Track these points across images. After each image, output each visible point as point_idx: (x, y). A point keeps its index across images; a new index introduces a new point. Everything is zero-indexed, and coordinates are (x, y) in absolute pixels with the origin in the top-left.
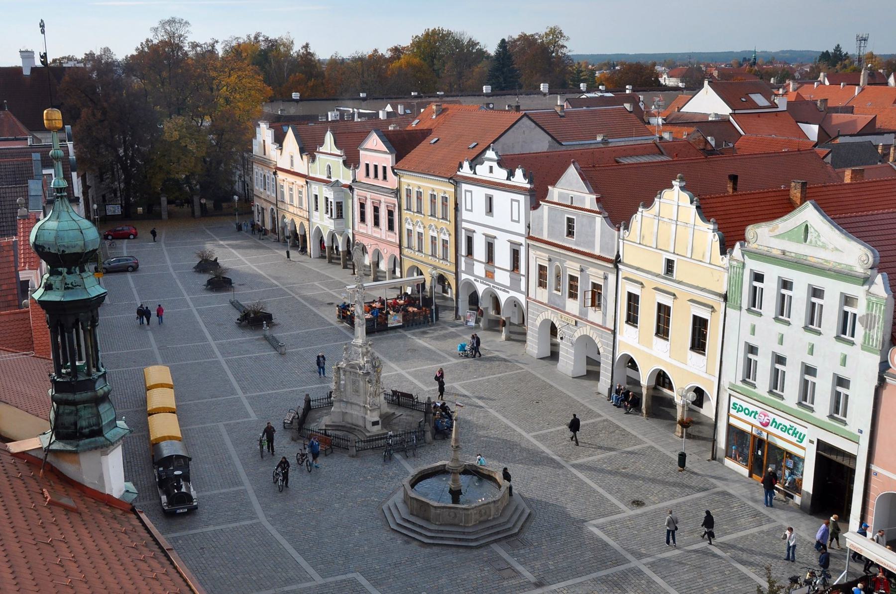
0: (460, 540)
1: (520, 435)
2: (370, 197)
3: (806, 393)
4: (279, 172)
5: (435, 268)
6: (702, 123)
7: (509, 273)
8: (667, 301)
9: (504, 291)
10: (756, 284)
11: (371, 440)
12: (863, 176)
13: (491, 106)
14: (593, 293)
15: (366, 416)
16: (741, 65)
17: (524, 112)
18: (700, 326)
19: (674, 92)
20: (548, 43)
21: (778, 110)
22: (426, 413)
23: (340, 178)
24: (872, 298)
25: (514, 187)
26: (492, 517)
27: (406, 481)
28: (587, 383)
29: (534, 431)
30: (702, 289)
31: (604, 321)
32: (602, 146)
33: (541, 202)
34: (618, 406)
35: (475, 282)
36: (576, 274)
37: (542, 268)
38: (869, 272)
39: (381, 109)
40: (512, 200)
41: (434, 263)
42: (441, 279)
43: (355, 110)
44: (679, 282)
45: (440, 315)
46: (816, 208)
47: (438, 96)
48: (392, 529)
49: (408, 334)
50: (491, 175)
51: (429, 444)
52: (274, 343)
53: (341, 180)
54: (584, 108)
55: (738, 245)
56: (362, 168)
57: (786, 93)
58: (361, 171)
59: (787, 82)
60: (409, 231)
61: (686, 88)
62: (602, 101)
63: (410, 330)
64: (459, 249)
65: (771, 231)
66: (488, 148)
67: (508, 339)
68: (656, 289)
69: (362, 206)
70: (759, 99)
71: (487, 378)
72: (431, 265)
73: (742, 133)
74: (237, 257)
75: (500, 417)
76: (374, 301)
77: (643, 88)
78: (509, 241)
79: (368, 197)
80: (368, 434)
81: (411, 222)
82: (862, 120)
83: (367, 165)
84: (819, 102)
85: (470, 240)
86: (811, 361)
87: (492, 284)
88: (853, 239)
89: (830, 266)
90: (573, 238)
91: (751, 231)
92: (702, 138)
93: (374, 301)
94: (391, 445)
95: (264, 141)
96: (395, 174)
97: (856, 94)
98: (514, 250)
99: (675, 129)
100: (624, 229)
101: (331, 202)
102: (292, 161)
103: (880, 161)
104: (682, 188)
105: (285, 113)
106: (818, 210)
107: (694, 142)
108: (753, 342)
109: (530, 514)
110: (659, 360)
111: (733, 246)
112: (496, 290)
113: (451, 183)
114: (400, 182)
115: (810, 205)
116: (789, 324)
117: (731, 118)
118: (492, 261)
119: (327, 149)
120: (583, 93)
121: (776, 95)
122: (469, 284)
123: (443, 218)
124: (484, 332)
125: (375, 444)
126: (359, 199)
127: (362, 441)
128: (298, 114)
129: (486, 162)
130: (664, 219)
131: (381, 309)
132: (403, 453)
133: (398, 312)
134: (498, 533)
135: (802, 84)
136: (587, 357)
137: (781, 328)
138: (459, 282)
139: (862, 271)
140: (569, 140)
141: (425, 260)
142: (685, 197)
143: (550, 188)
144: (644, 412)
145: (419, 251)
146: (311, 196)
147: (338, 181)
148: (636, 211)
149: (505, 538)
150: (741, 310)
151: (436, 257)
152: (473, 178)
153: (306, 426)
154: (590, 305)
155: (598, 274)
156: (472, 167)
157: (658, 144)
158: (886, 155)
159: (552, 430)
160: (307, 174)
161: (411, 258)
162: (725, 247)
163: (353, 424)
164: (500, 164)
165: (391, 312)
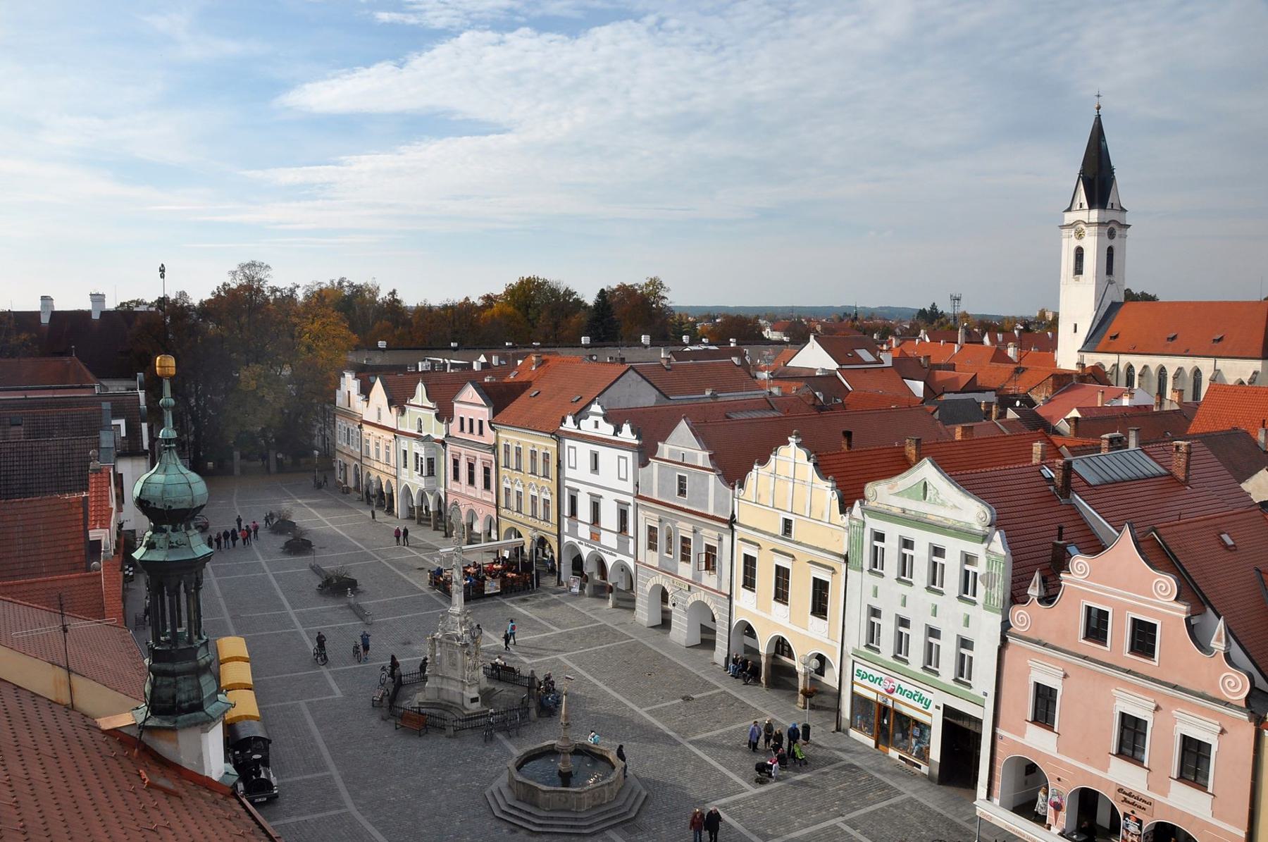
0: (572, 827)
2: (465, 453)
3: (931, 655)
4: (364, 425)
5: (536, 529)
6: (808, 377)
7: (616, 535)
8: (785, 563)
9: (611, 554)
10: (876, 543)
11: (470, 718)
12: (972, 434)
13: (594, 358)
15: (464, 692)
16: (842, 320)
17: (630, 364)
18: (820, 588)
19: (778, 346)
20: (649, 294)
21: (884, 365)
22: (529, 688)
23: (432, 432)
24: (991, 556)
26: (606, 801)
27: (511, 764)
28: (701, 652)
29: (648, 705)
31: (720, 585)
32: (712, 401)
33: (650, 459)
34: (735, 676)
35: (579, 545)
36: (689, 536)
38: (988, 530)
39: (475, 360)
40: (619, 457)
41: (535, 525)
42: (542, 542)
43: (446, 360)
44: (798, 543)
45: (541, 581)
46: (933, 465)
47: (534, 347)
48: (497, 817)
49: (507, 602)
50: (596, 430)
51: (534, 722)
54: (691, 361)
55: (857, 503)
56: (456, 423)
57: (890, 349)
58: (455, 425)
59: (890, 338)
60: (507, 490)
61: (791, 342)
63: (510, 597)
65: (889, 488)
66: (593, 401)
67: (615, 606)
68: (773, 550)
69: (456, 462)
70: (865, 354)
71: (594, 648)
72: (531, 527)
73: (850, 389)
75: (609, 691)
76: (469, 566)
78: (616, 500)
79: (463, 453)
80: (466, 712)
81: (509, 480)
82: (964, 377)
83: (462, 419)
84: (922, 359)
85: (573, 500)
86: (934, 623)
87: (597, 547)
88: (970, 496)
89: (950, 523)
91: (870, 489)
94: (492, 724)
95: (349, 392)
96: (493, 429)
97: (956, 352)
98: (621, 510)
99: (785, 384)
100: (739, 488)
102: (379, 414)
103: (985, 419)
105: (370, 363)
106: (936, 467)
108: (876, 605)
109: (646, 797)
111: (852, 505)
112: (602, 553)
114: (497, 437)
115: (928, 462)
116: (911, 584)
117: (838, 373)
120: (686, 345)
121: (881, 351)
122: (573, 547)
123: (544, 476)
126: (453, 455)
127: (460, 720)
129: (590, 417)
130: (781, 477)
131: (476, 575)
132: (505, 732)
133: (493, 577)
134: (614, 818)
135: (903, 341)
136: (701, 625)
137: (904, 589)
138: (562, 545)
139: (980, 528)
142: (802, 454)
143: (659, 444)
144: (763, 681)
145: (517, 511)
146: (400, 452)
147: (429, 435)
148: (751, 469)
150: (862, 572)
151: (536, 518)
154: (704, 568)
157: (769, 399)
158: (988, 413)
160: (395, 428)
161: (509, 519)
162: (845, 506)
163: (449, 702)
164: (607, 419)
165: (488, 578)
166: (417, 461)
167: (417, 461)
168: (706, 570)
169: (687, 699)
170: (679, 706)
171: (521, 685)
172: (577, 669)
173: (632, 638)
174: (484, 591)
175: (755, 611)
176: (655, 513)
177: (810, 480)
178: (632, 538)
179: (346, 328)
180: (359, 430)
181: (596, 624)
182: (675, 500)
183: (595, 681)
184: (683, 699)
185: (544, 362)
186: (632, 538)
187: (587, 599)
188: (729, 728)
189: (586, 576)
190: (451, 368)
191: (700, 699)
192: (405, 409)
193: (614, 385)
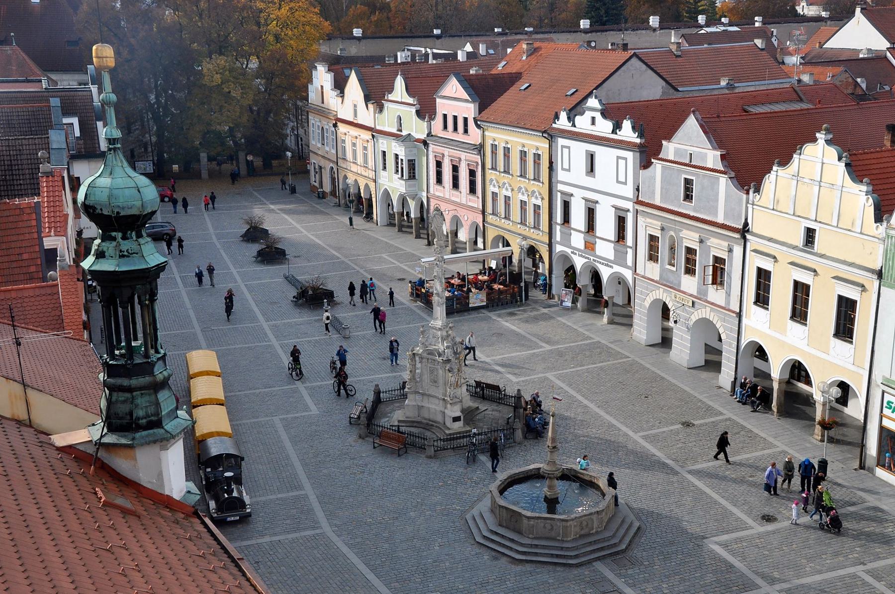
0: (557, 556)
1: (626, 435)
2: (448, 155)
4: (339, 124)
5: (525, 238)
8: (805, 278)
9: (607, 265)
11: (452, 438)
13: (593, 44)
14: (715, 269)
15: (446, 411)
22: (516, 408)
25: (621, 142)
26: (594, 530)
27: (494, 487)
28: (704, 375)
29: (643, 430)
31: (728, 301)
32: (727, 92)
33: (653, 160)
35: (572, 255)
36: (695, 246)
37: (653, 239)
39: (460, 49)
40: (618, 158)
41: (524, 233)
42: (532, 251)
43: (428, 50)
44: (822, 256)
47: (527, 33)
49: (493, 315)
50: (593, 127)
53: (413, 134)
56: (439, 121)
58: (438, 123)
60: (494, 195)
61: (831, 18)
62: (726, 36)
63: (494, 311)
64: (554, 215)
66: (590, 95)
67: (611, 322)
68: (792, 263)
69: (439, 164)
72: (520, 235)
74: (291, 223)
75: (602, 413)
76: (452, 278)
77: (777, 20)
79: (446, 154)
80: (447, 432)
83: (445, 116)
85: (566, 206)
87: (592, 258)
90: (692, 203)
92: (850, 80)
93: (452, 278)
94: (474, 445)
95: (322, 87)
96: (478, 126)
98: (619, 217)
99: (818, 69)
100: (754, 193)
101: (402, 160)
102: (355, 111)
104: (829, 142)
105: (345, 54)
109: (639, 528)
110: (794, 349)
112: (598, 264)
113: (545, 137)
114: (483, 136)
118: (593, 230)
120: (701, 27)
122: (565, 258)
123: (534, 179)
124: (583, 313)
127: (441, 440)
128: (360, 54)
129: (587, 112)
130: (805, 180)
131: (461, 287)
133: (480, 289)
134: (602, 549)
136: (706, 345)
138: (554, 254)
140: (686, 85)
141: (513, 229)
142: (832, 153)
143: (664, 142)
145: (505, 218)
147: (410, 134)
148: (769, 171)
149: (611, 555)
151: (526, 225)
152: (571, 131)
155: (721, 245)
156: (570, 119)
157: (797, 89)
159: (665, 429)
160: (373, 127)
161: (496, 226)
163: (430, 420)
164: (605, 114)
165: (473, 290)
166: (397, 163)
167: (397, 163)
168: (713, 284)
169: (687, 425)
170: (677, 433)
171: (507, 405)
172: (567, 388)
173: (629, 357)
175: (768, 332)
178: (631, 248)
179: (317, 14)
181: (589, 341)
182: (680, 206)
183: (586, 402)
184: (683, 424)
185: (536, 50)
186: (631, 248)
187: (579, 315)
189: (580, 289)
191: (701, 425)
192: (383, 105)
193: (614, 76)
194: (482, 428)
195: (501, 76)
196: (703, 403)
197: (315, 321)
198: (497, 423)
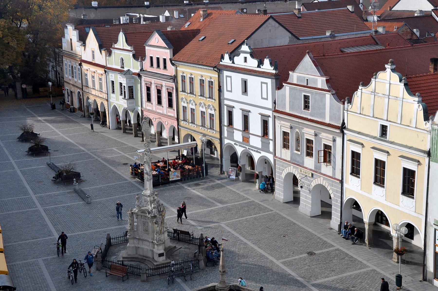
1: (272, 262)
2: (154, 82)
4: (83, 64)
5: (204, 135)
7: (260, 138)
8: (382, 157)
9: (257, 152)
11: (158, 268)
13: (245, 11)
15: (154, 250)
22: (200, 246)
25: (263, 72)
28: (321, 221)
29: (282, 258)
30: (410, 148)
31: (334, 173)
32: (330, 39)
33: (284, 84)
35: (235, 146)
36: (312, 138)
37: (285, 134)
39: (161, 14)
40: (262, 83)
41: (204, 132)
42: (209, 144)
43: (141, 15)
44: (392, 143)
45: (209, 171)
47: (205, 4)
49: (185, 186)
50: (245, 64)
52: (82, 195)
53: (131, 69)
54: (316, 10)
56: (148, 60)
58: (147, 63)
63: (186, 183)
64: (222, 121)
66: (243, 43)
68: (373, 148)
69: (148, 89)
72: (201, 133)
74: (52, 129)
75: (256, 248)
76: (159, 162)
79: (153, 82)
80: (155, 264)
83: (151, 58)
85: (230, 114)
87: (247, 147)
90: (309, 110)
92: (409, 30)
93: (159, 162)
94: (173, 272)
96: (173, 64)
99: (388, 24)
100: (348, 103)
101: (124, 87)
102: (93, 55)
104: (393, 70)
105: (87, 18)
107: (403, 34)
110: (377, 203)
112: (251, 151)
114: (176, 71)
119: (120, 46)
122: (231, 147)
123: (210, 98)
125: (161, 271)
126: (146, 84)
127: (151, 269)
128: (96, 18)
129: (241, 54)
130: (379, 95)
131: (164, 168)
132: (183, 277)
133: (175, 169)
136: (321, 201)
142: (395, 77)
143: (290, 73)
145: (192, 123)
147: (129, 70)
148: (357, 89)
151: (205, 127)
153: (108, 259)
154: (322, 161)
156: (231, 58)
157: (374, 37)
159: (297, 257)
160: (105, 65)
161: (186, 128)
163: (144, 256)
165: (172, 170)
166: (121, 89)
167: (121, 89)
169: (311, 254)
170: (304, 259)
171: (194, 244)
172: (233, 232)
173: (272, 211)
174: (169, 179)
175: (360, 192)
176: (288, 122)
177: (401, 96)
178: (272, 140)
180: (79, 67)
181: (247, 201)
182: (301, 113)
183: (245, 241)
184: (308, 253)
186: (272, 140)
187: (241, 184)
188: (340, 276)
189: (240, 167)
190: (144, 21)
191: (320, 254)
192: (111, 51)
193: (259, 31)
194: (178, 260)
195: (187, 32)
196: (321, 239)
197: (68, 193)
198: (188, 257)
